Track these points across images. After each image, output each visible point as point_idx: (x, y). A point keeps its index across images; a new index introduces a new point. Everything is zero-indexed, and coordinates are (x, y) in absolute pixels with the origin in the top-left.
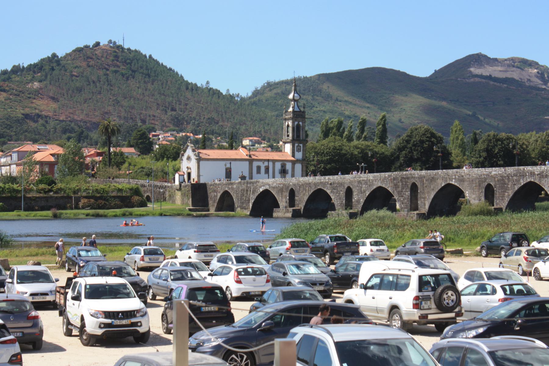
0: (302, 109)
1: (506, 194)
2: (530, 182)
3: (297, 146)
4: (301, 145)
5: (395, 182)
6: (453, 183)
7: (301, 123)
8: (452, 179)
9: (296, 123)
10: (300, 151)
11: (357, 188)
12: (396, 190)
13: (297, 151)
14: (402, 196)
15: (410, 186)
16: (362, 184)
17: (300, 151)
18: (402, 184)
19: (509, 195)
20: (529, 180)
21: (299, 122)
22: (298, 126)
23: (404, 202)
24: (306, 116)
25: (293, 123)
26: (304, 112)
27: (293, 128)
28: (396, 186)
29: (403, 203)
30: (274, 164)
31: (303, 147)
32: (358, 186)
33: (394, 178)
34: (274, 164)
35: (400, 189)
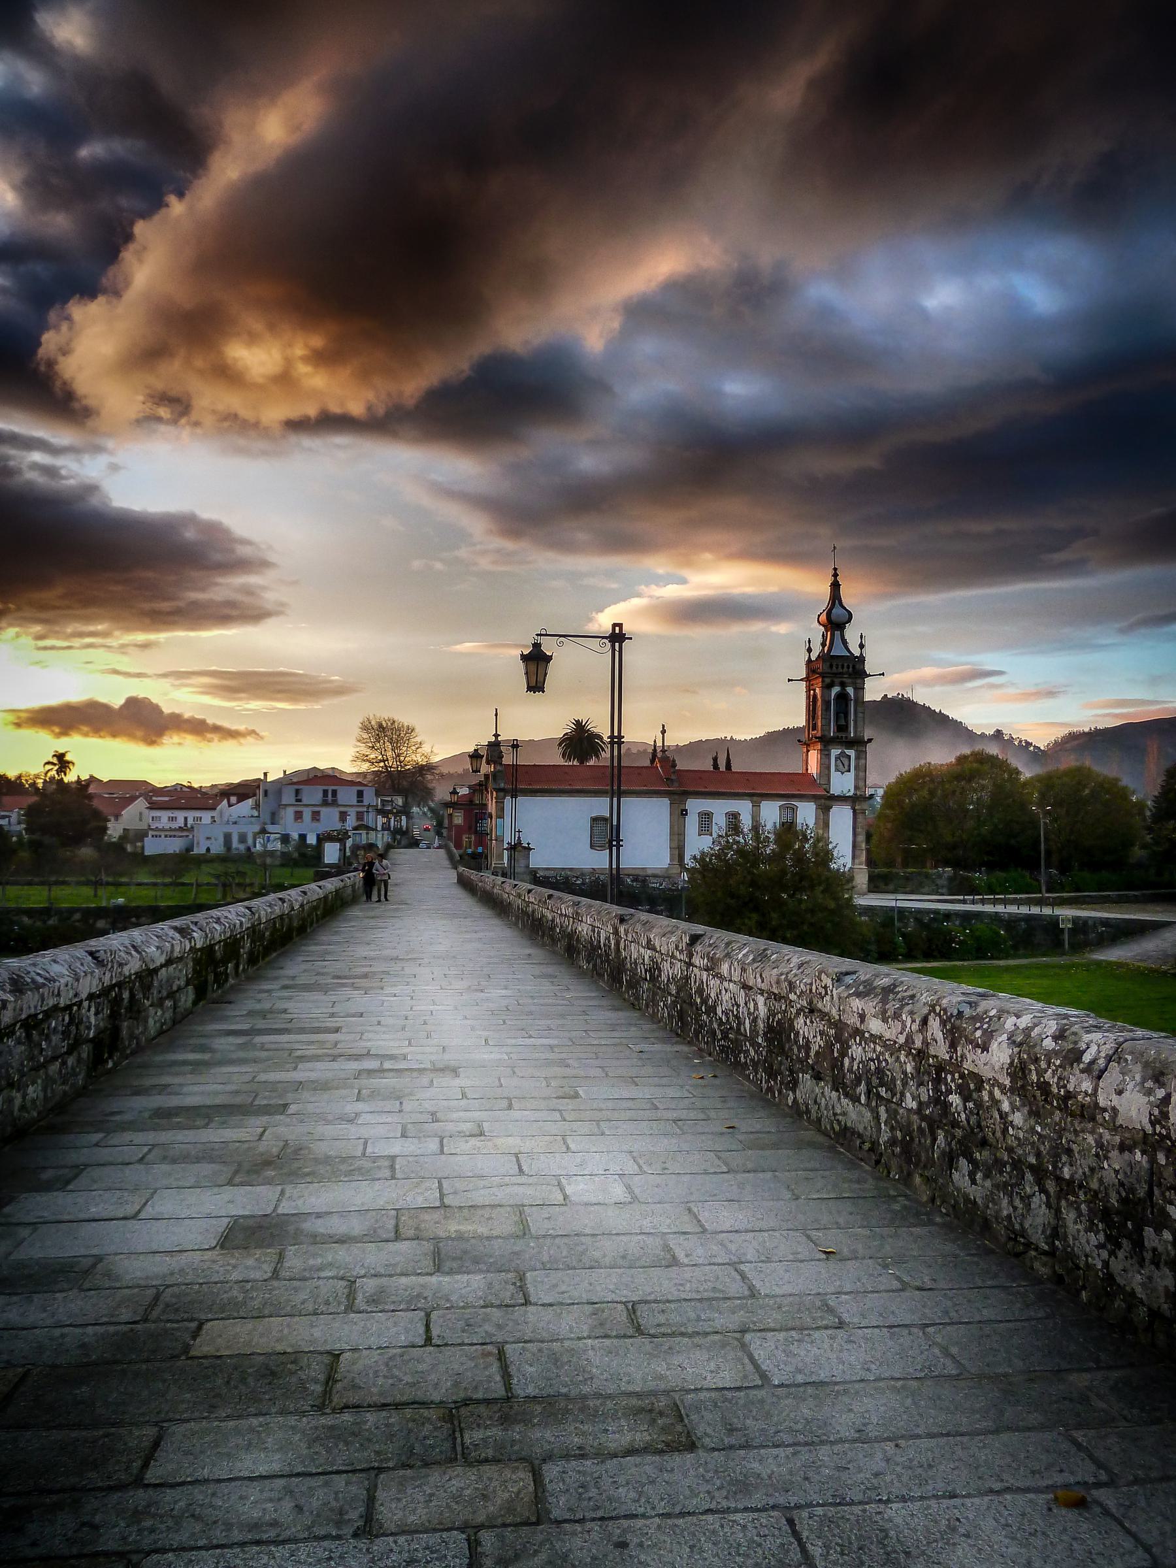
0: (856, 652)
3: (837, 758)
4: (852, 753)
7: (850, 690)
9: (836, 690)
10: (849, 771)
13: (837, 770)
17: (849, 771)
21: (843, 685)
22: (842, 697)
24: (868, 668)
25: (828, 687)
26: (862, 659)
27: (827, 704)
30: (756, 805)
31: (857, 758)
34: (756, 805)
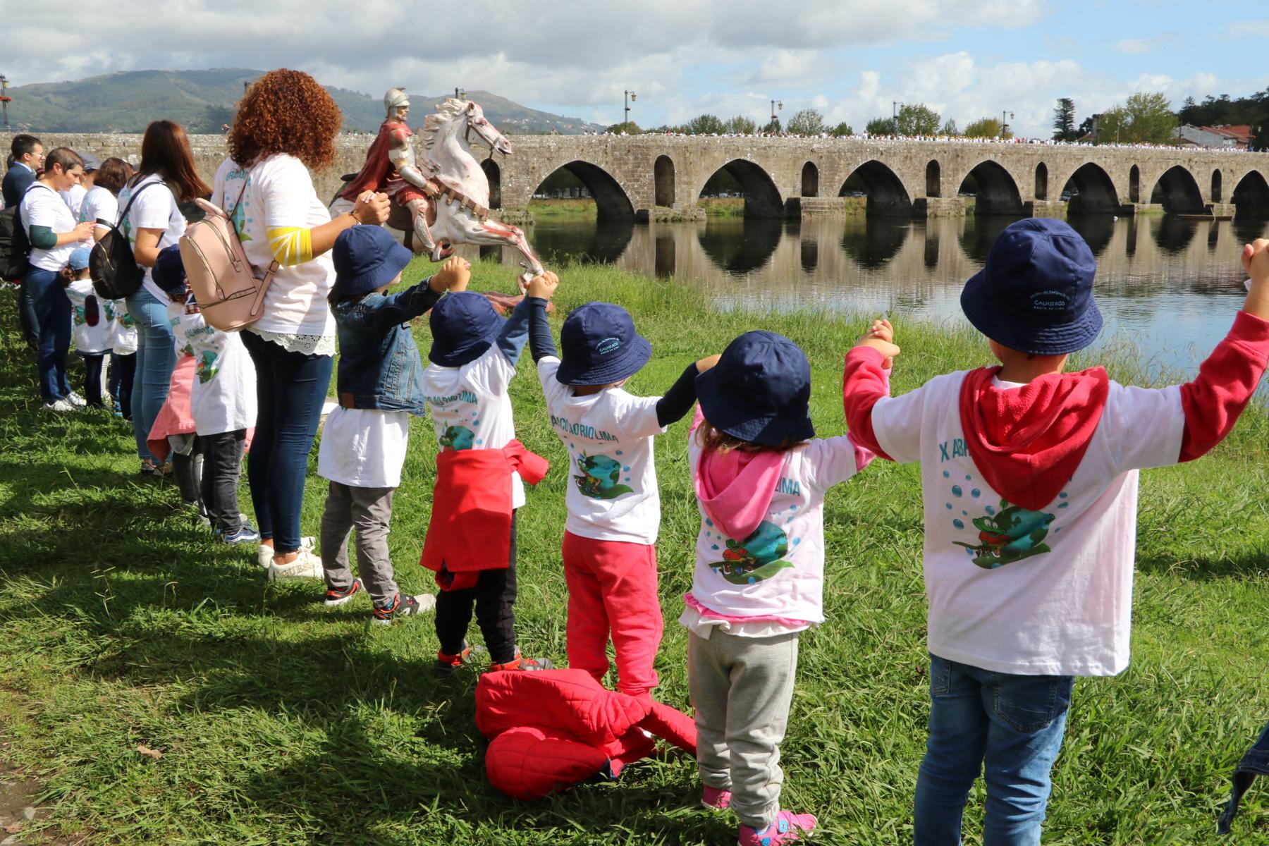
1: (837, 178)
2: (873, 161)
5: (617, 153)
6: (748, 159)
8: (748, 152)
11: (514, 163)
12: (619, 168)
14: (637, 180)
15: (653, 162)
16: (527, 155)
18: (636, 158)
19: (841, 180)
20: (870, 159)
23: (641, 191)
28: (620, 161)
29: (638, 193)
32: (516, 160)
33: (612, 146)
35: (630, 167)
